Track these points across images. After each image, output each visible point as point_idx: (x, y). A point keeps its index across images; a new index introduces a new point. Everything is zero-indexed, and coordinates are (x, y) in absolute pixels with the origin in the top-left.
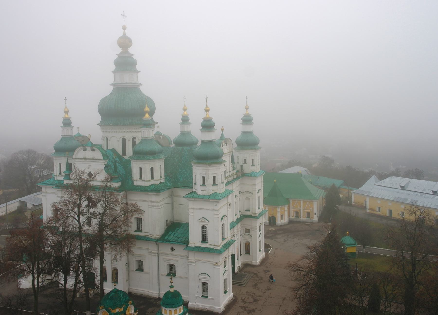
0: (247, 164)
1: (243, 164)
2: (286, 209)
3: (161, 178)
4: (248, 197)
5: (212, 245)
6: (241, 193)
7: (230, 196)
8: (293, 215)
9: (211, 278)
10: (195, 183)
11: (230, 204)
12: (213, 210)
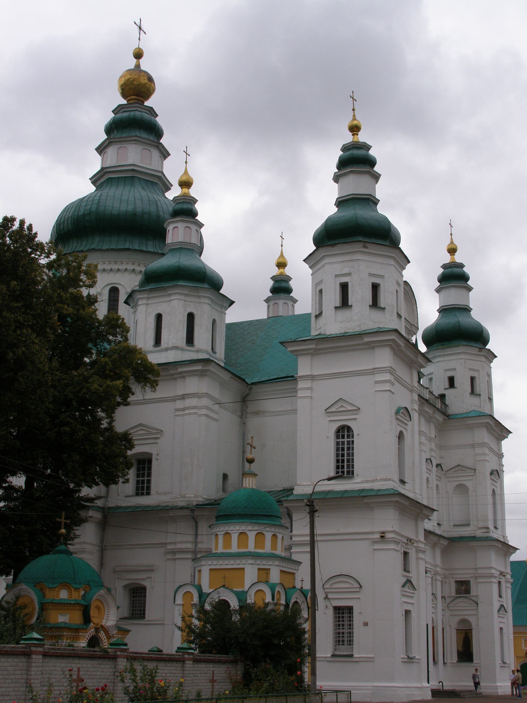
0: (456, 388)
1: (445, 389)
4: (464, 483)
5: (367, 481)
6: (439, 467)
9: (363, 588)
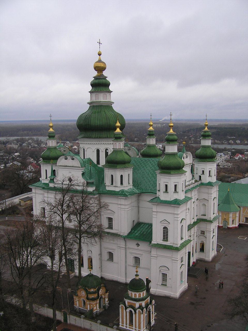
2: (237, 215)
3: (130, 185)
7: (189, 202)
8: (243, 221)
10: (159, 190)
11: (189, 209)
12: (174, 214)
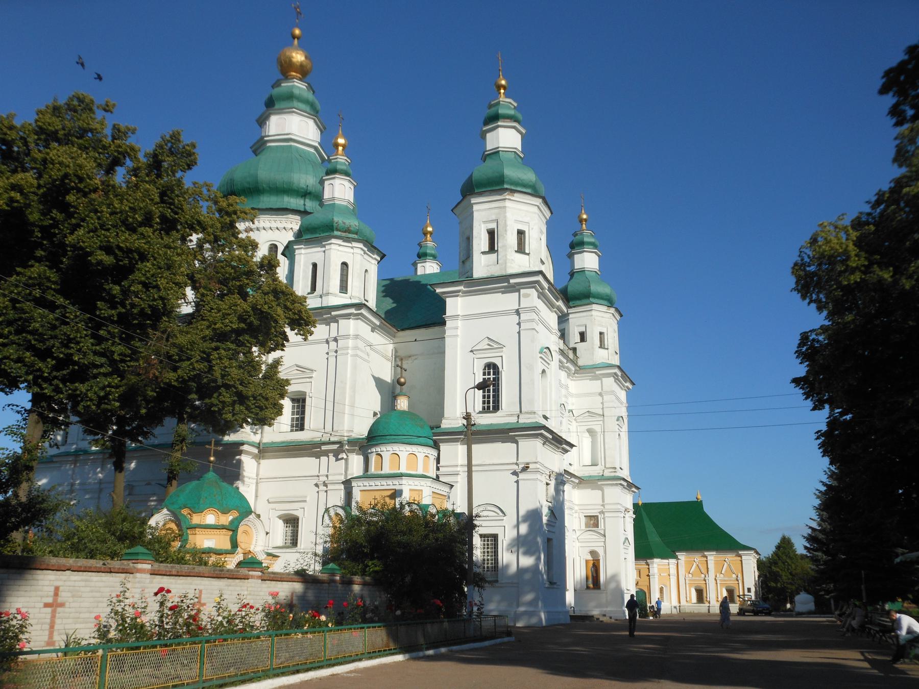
2: (673, 571)
